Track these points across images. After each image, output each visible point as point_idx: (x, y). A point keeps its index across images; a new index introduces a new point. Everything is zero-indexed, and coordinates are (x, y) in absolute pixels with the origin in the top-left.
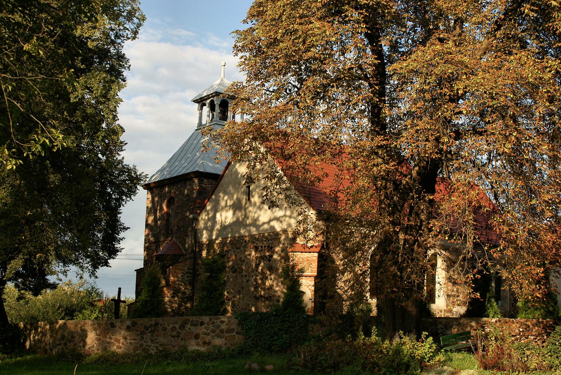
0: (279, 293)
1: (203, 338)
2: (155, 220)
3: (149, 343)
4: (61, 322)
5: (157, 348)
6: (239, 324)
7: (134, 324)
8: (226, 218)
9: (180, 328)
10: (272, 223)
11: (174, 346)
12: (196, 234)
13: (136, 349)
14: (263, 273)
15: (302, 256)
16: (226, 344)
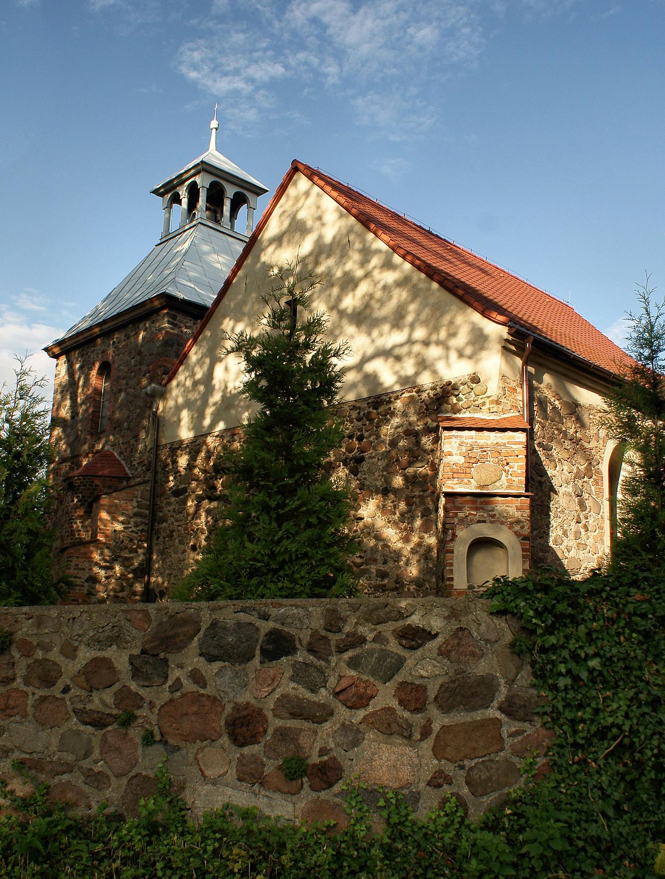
1: (283, 734)
9: (136, 672)
10: (369, 367)
11: (97, 780)
15: (482, 442)
16: (437, 781)
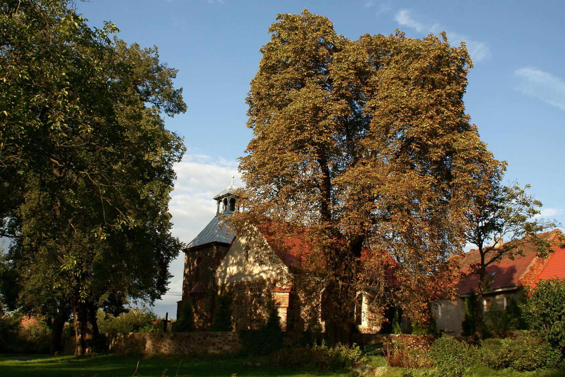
0: (265, 318)
2: (190, 271)
3: (184, 348)
4: (131, 333)
5: (189, 351)
6: (240, 337)
7: (175, 336)
8: (233, 271)
10: (261, 274)
11: (199, 350)
12: (215, 280)
13: (176, 351)
14: (255, 305)
16: (231, 349)
